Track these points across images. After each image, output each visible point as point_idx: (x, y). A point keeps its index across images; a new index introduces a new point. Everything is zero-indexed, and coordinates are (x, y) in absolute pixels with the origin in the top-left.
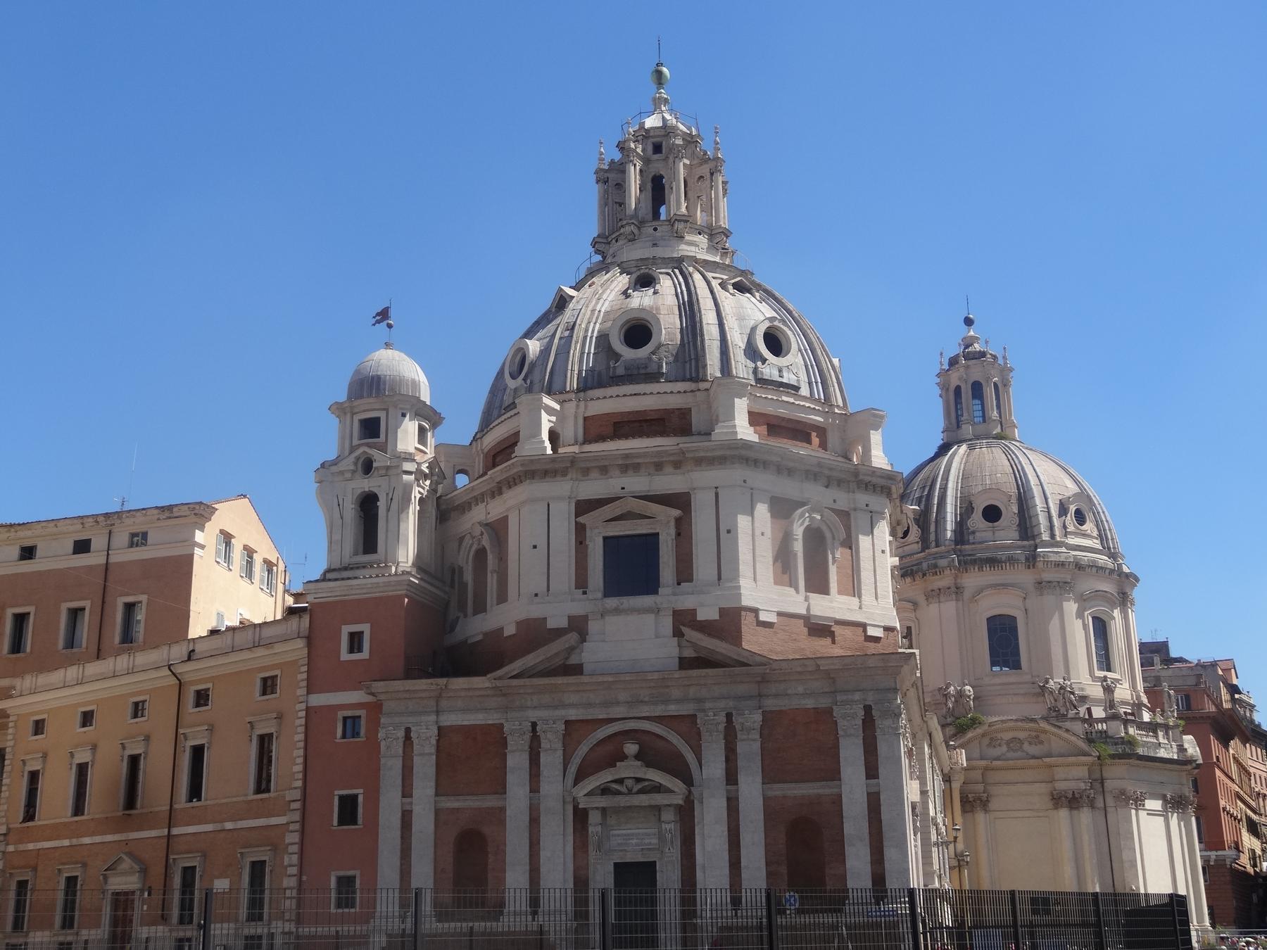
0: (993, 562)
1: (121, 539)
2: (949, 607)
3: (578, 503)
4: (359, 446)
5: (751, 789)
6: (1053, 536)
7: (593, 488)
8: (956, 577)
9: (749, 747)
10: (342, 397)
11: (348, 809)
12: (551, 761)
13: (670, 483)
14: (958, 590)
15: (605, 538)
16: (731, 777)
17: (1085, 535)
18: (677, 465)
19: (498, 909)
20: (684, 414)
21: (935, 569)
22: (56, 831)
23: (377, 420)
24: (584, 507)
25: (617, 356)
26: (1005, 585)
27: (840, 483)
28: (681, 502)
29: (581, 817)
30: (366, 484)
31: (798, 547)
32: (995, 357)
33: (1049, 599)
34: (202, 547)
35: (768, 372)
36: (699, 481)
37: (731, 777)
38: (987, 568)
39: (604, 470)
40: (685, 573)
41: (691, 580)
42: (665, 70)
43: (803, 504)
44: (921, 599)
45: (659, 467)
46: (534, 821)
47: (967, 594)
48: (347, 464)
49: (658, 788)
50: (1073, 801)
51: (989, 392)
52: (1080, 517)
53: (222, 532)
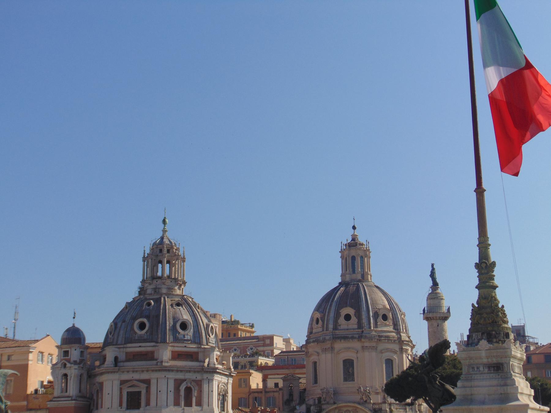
0: (345, 338)
2: (329, 356)
3: (121, 381)
4: (63, 359)
6: (370, 327)
7: (125, 377)
8: (332, 344)
10: (59, 344)
13: (145, 376)
14: (332, 348)
15: (128, 393)
17: (386, 325)
18: (147, 371)
20: (152, 353)
21: (324, 341)
23: (68, 351)
24: (123, 382)
25: (136, 333)
26: (349, 348)
27: (198, 372)
28: (147, 382)
30: (64, 371)
31: (182, 393)
32: (362, 244)
33: (367, 354)
34: (32, 360)
35: (180, 337)
36: (153, 376)
38: (342, 341)
39: (128, 372)
40: (148, 403)
41: (149, 405)
42: (167, 220)
43: (185, 380)
44: (320, 351)
45: (143, 371)
47: (336, 351)
48: (59, 365)
53: (39, 352)
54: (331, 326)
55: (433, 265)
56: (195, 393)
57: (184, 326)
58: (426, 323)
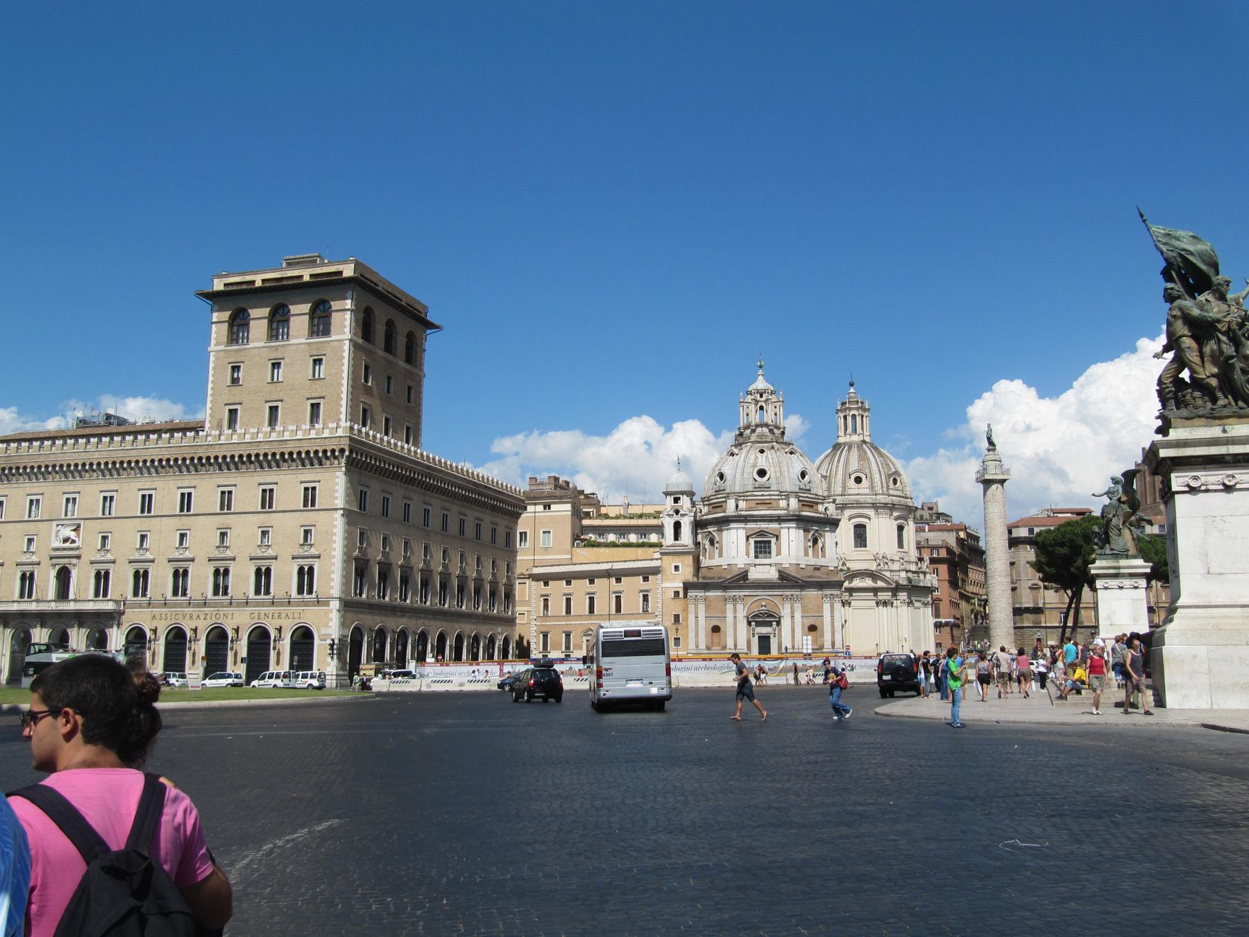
1: (540, 508)
5: (798, 615)
9: (798, 606)
11: (677, 618)
12: (740, 607)
16: (792, 612)
19: (725, 647)
22: (558, 617)
29: (749, 623)
31: (810, 544)
37: (792, 612)
40: (779, 553)
45: (771, 521)
46: (735, 624)
49: (771, 616)
50: (885, 603)
51: (859, 419)
52: (895, 481)
54: (839, 490)
55: (989, 426)
56: (820, 544)
57: (803, 475)
58: (981, 486)
